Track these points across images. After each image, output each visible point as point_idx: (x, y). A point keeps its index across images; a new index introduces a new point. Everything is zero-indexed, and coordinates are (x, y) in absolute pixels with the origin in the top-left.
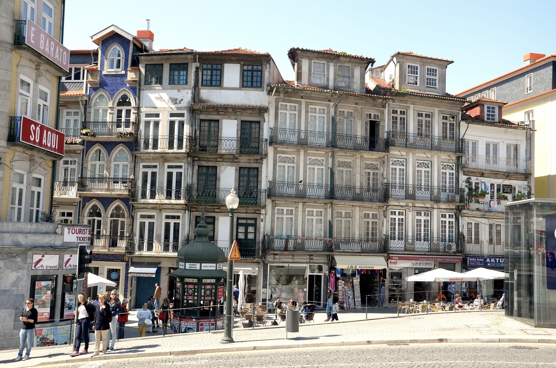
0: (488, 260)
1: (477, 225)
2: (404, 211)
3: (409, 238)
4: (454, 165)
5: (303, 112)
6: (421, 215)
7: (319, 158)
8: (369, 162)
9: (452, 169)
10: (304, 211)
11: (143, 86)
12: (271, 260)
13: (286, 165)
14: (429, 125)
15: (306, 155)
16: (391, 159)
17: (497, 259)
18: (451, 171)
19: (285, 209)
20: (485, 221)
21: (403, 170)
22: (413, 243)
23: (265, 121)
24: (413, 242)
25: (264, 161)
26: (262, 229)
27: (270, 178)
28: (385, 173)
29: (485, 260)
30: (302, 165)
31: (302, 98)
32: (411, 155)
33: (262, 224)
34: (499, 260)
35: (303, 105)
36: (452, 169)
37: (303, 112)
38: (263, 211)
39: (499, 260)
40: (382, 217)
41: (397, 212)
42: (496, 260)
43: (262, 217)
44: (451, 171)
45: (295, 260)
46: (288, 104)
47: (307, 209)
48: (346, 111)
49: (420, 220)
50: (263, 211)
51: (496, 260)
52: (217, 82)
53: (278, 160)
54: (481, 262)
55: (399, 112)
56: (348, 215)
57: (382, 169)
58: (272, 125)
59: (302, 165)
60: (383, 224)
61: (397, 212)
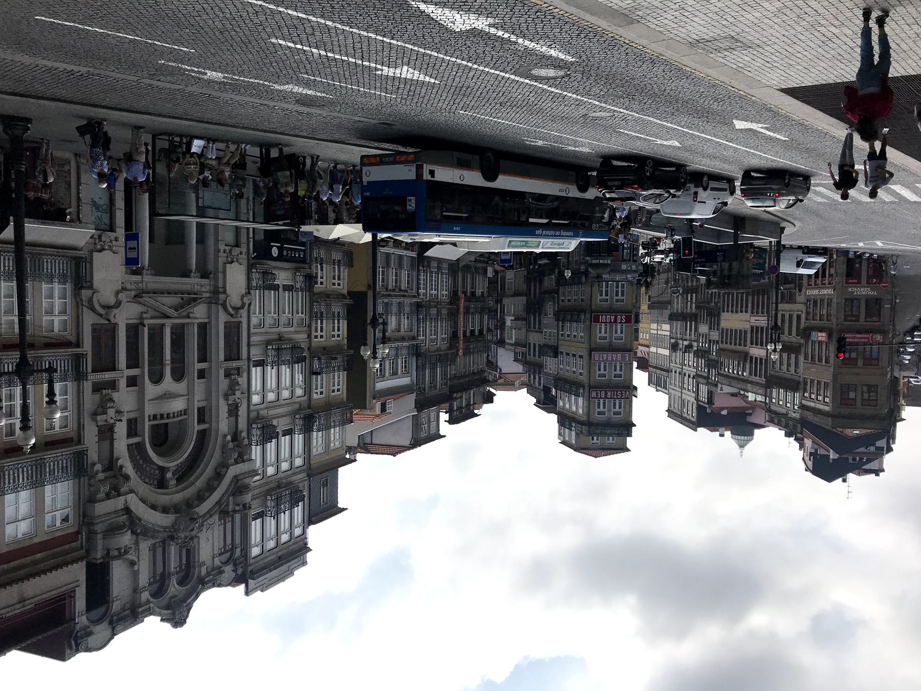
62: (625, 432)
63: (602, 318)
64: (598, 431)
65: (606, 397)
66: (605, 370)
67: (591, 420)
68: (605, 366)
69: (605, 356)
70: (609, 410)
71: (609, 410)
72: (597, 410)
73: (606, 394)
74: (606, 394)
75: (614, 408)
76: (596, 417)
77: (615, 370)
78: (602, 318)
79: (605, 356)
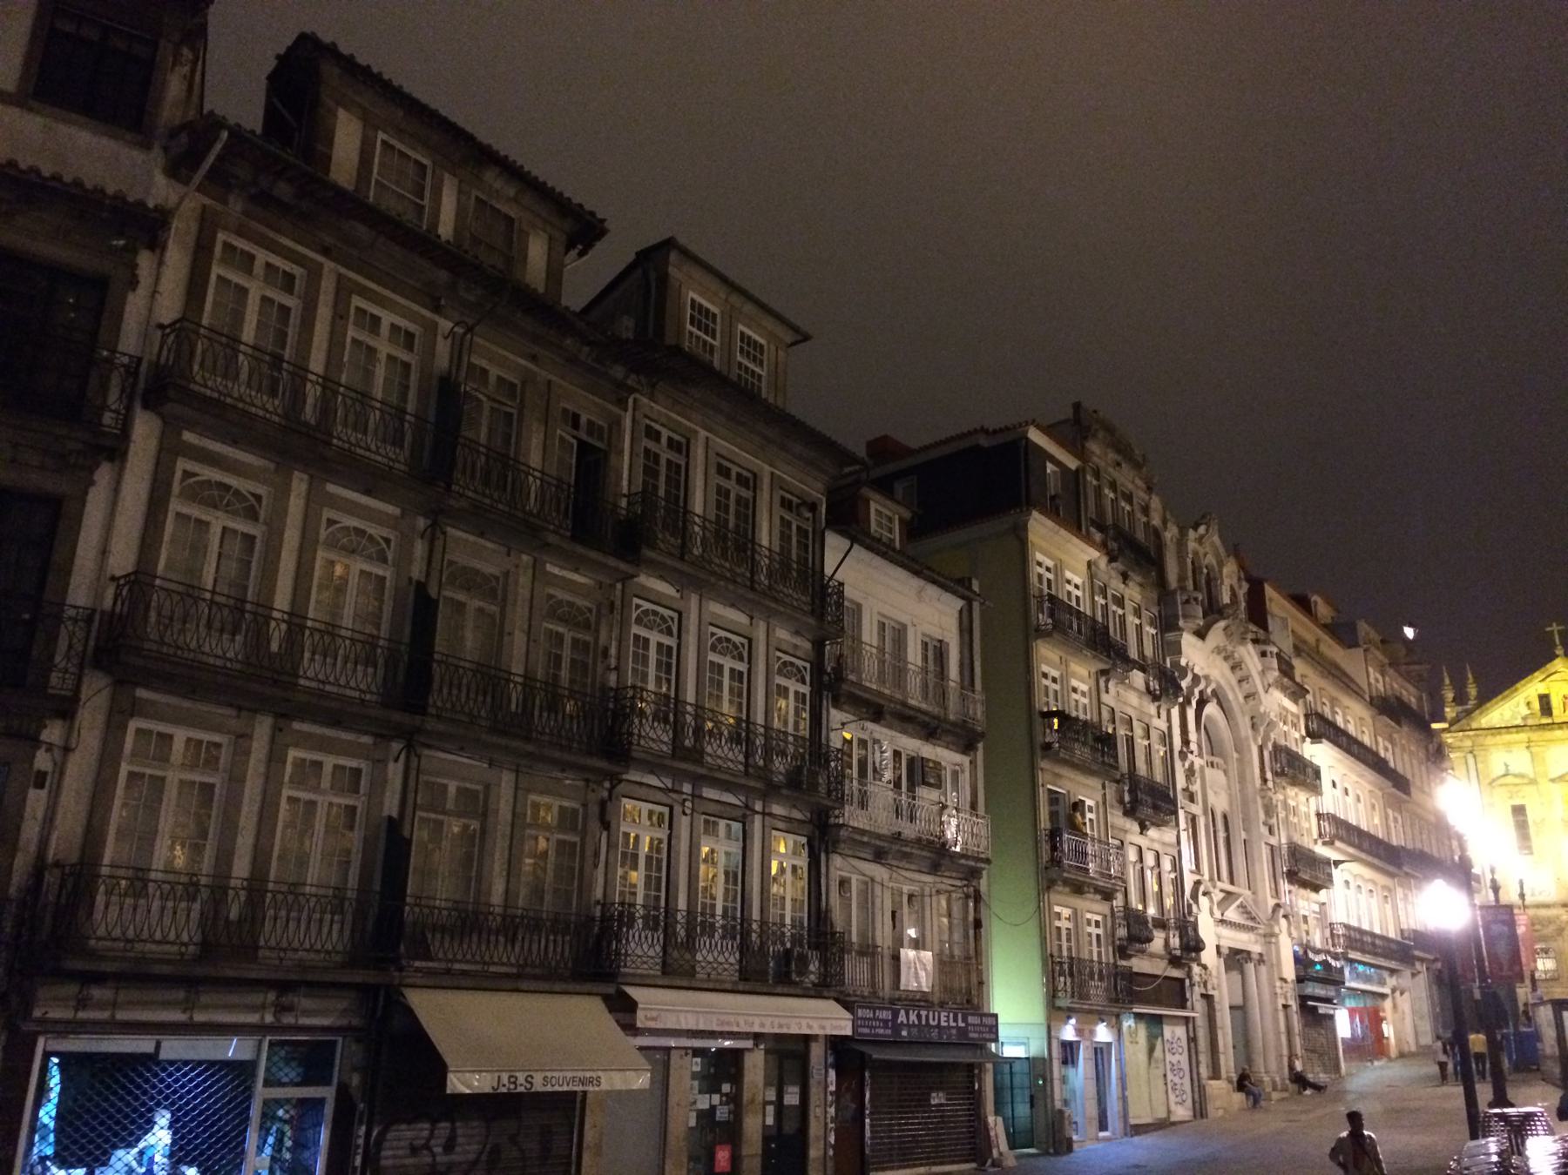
2: (666, 810)
3: (679, 917)
4: (808, 665)
5: (324, 313)
7: (373, 530)
10: (275, 758)
13: (218, 521)
14: (747, 511)
15: (314, 500)
16: (636, 601)
21: (670, 648)
22: (690, 945)
23: (133, 283)
24: (690, 935)
25: (104, 474)
26: (30, 832)
27: (122, 560)
28: (613, 651)
30: (291, 537)
31: (326, 251)
32: (694, 600)
33: (37, 799)
35: (327, 286)
37: (324, 313)
38: (53, 733)
40: (594, 825)
43: (42, 761)
45: (200, 1017)
47: (293, 754)
50: (53, 733)
53: (176, 488)
58: (169, 308)
59: (291, 537)
60: (597, 854)
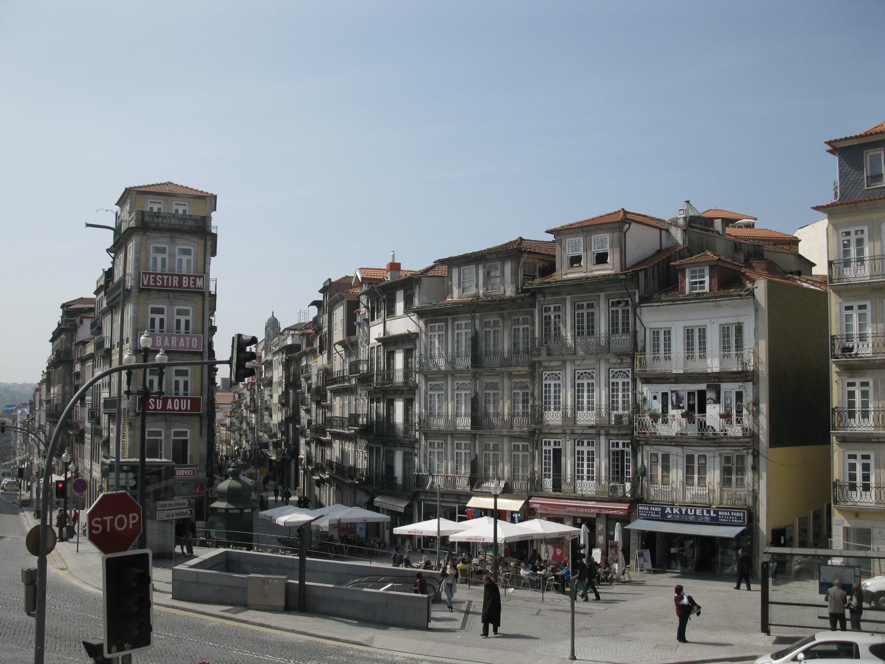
0: (668, 510)
1: (666, 457)
6: (583, 445)
8: (517, 380)
9: (628, 376)
11: (371, 323)
12: (423, 498)
17: (684, 510)
18: (626, 380)
19: (436, 442)
20: (678, 450)
29: (664, 509)
34: (686, 512)
36: (628, 376)
39: (686, 512)
41: (552, 441)
42: (680, 511)
44: (626, 380)
46: (437, 325)
47: (456, 442)
48: (492, 320)
49: (583, 452)
51: (680, 511)
52: (391, 312)
54: (657, 513)
55: (552, 309)
56: (496, 447)
57: (531, 387)
61: (552, 441)
62: (147, 219)
63: (185, 405)
64: (190, 223)
65: (181, 277)
66: (178, 321)
67: (201, 242)
68: (178, 327)
69: (182, 344)
70: (172, 255)
71: (172, 255)
72: (191, 258)
73: (180, 282)
74: (180, 282)
75: (164, 260)
76: (193, 245)
77: (162, 321)
78: (185, 405)
79: (182, 344)
